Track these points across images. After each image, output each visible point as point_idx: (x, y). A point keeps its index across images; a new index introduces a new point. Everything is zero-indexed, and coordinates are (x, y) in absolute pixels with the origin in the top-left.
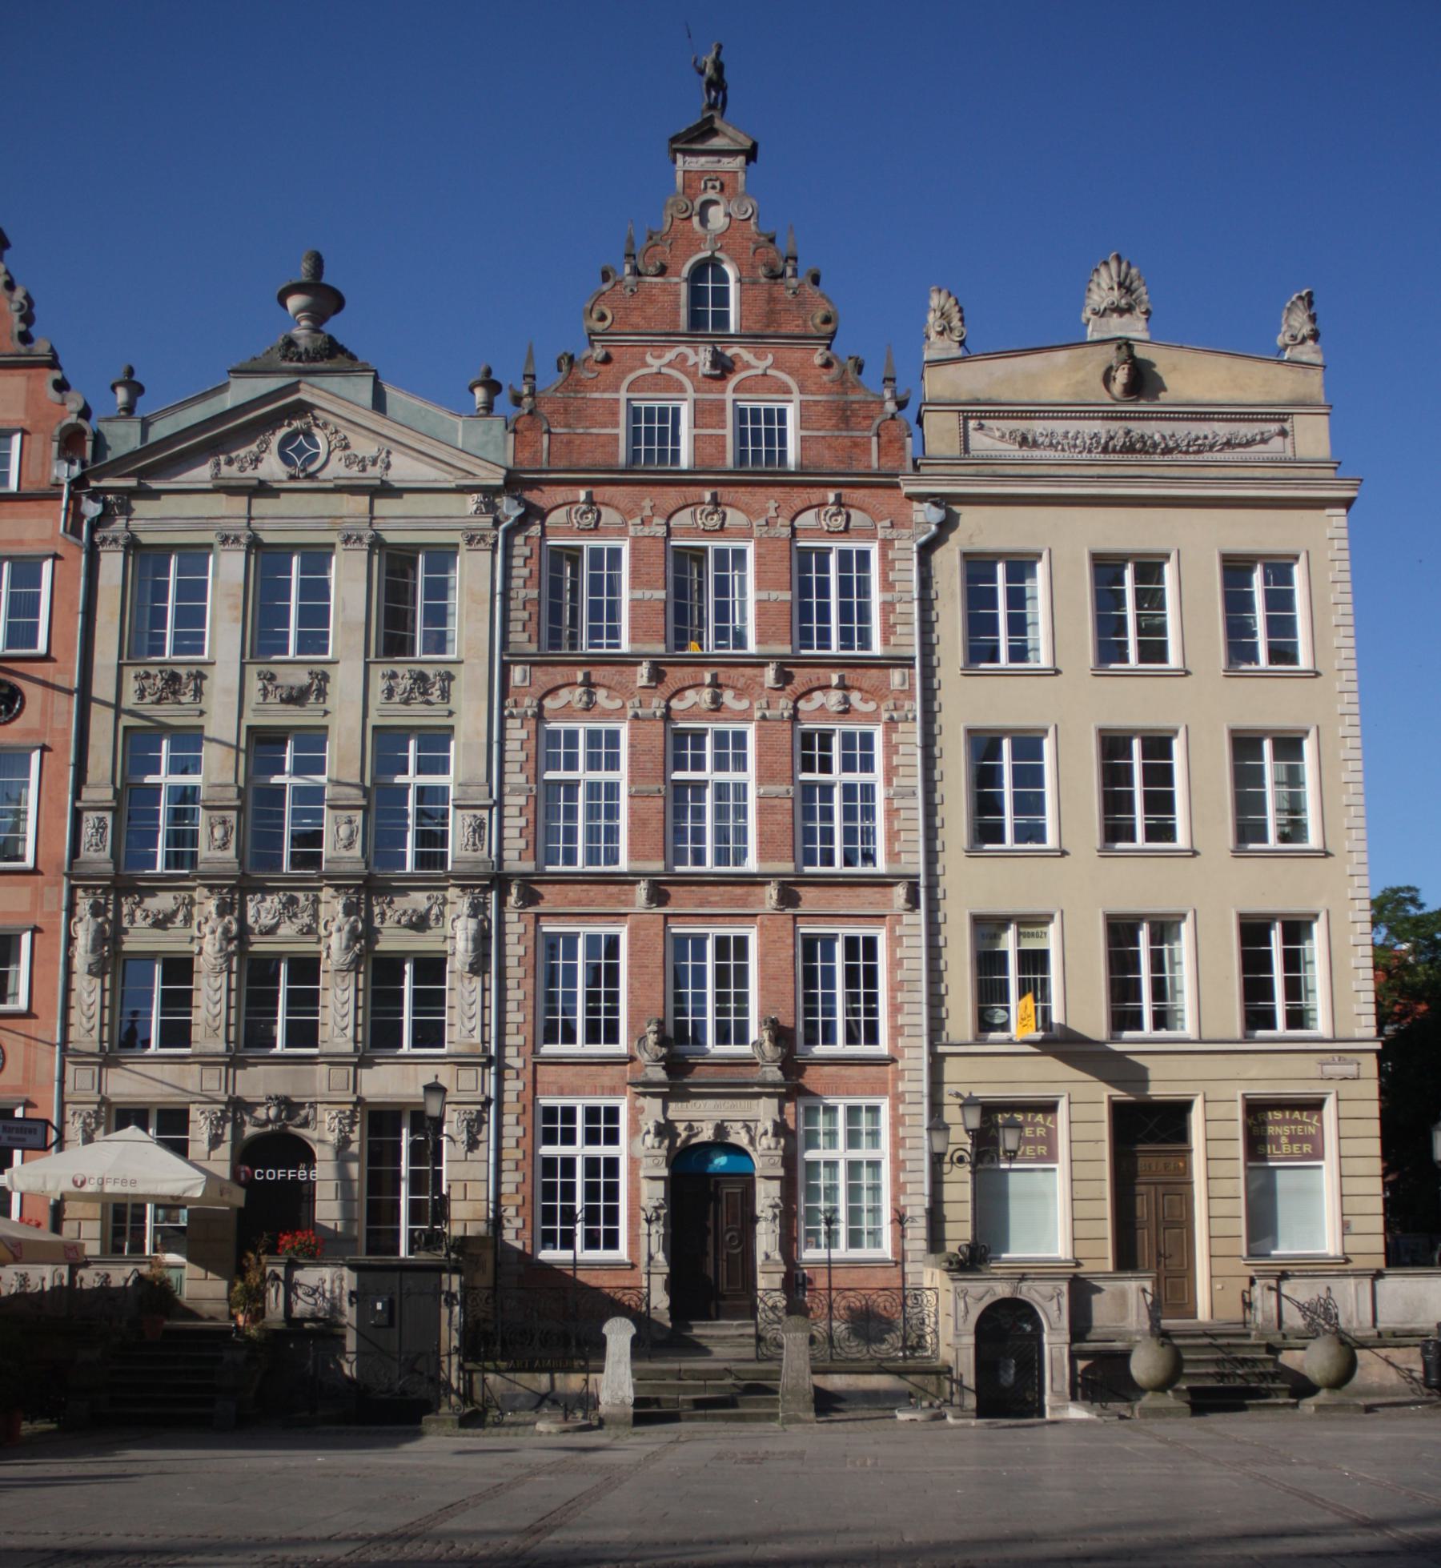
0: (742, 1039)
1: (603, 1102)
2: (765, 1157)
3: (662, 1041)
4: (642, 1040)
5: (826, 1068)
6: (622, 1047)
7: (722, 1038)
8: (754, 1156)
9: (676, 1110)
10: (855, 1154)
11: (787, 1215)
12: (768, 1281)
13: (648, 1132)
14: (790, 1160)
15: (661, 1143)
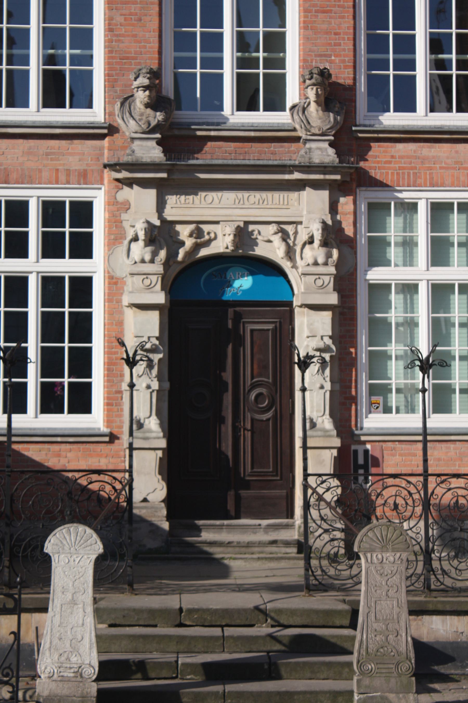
0: (275, 102)
1: (68, 194)
2: (309, 278)
3: (156, 103)
4: (127, 100)
5: (400, 146)
6: (97, 114)
7: (247, 102)
8: (292, 275)
9: (179, 207)
10: (442, 274)
11: (342, 364)
12: (315, 460)
13: (136, 239)
14: (346, 282)
15: (155, 254)
